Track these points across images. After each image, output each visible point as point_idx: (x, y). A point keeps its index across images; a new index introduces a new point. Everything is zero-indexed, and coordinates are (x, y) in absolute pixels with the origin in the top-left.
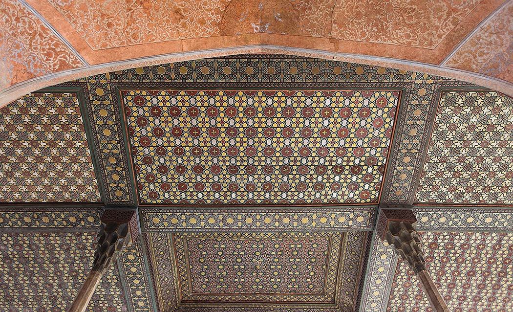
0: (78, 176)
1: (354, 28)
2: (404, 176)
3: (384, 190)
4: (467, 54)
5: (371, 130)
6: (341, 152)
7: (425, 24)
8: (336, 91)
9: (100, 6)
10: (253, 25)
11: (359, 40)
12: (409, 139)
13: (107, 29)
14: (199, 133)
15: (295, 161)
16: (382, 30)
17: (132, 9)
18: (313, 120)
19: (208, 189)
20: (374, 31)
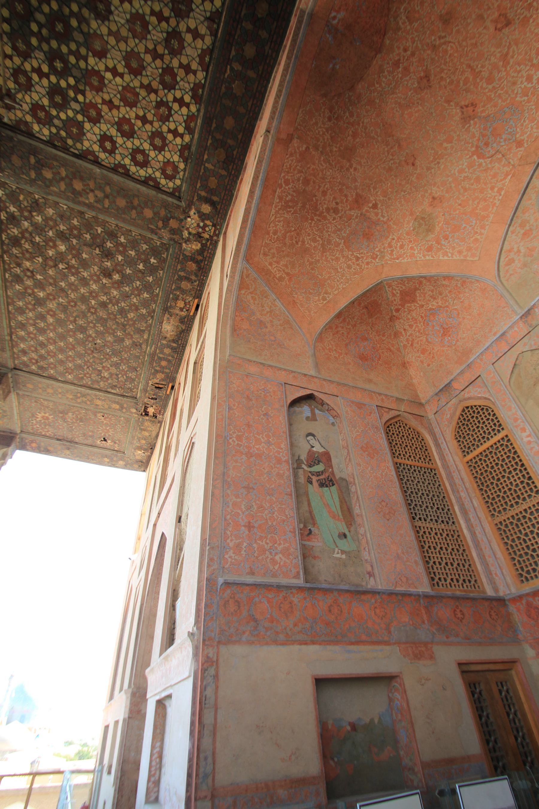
1: (296, 172)
4: (254, 286)
7: (283, 251)
11: (283, 175)
16: (286, 207)
20: (287, 196)
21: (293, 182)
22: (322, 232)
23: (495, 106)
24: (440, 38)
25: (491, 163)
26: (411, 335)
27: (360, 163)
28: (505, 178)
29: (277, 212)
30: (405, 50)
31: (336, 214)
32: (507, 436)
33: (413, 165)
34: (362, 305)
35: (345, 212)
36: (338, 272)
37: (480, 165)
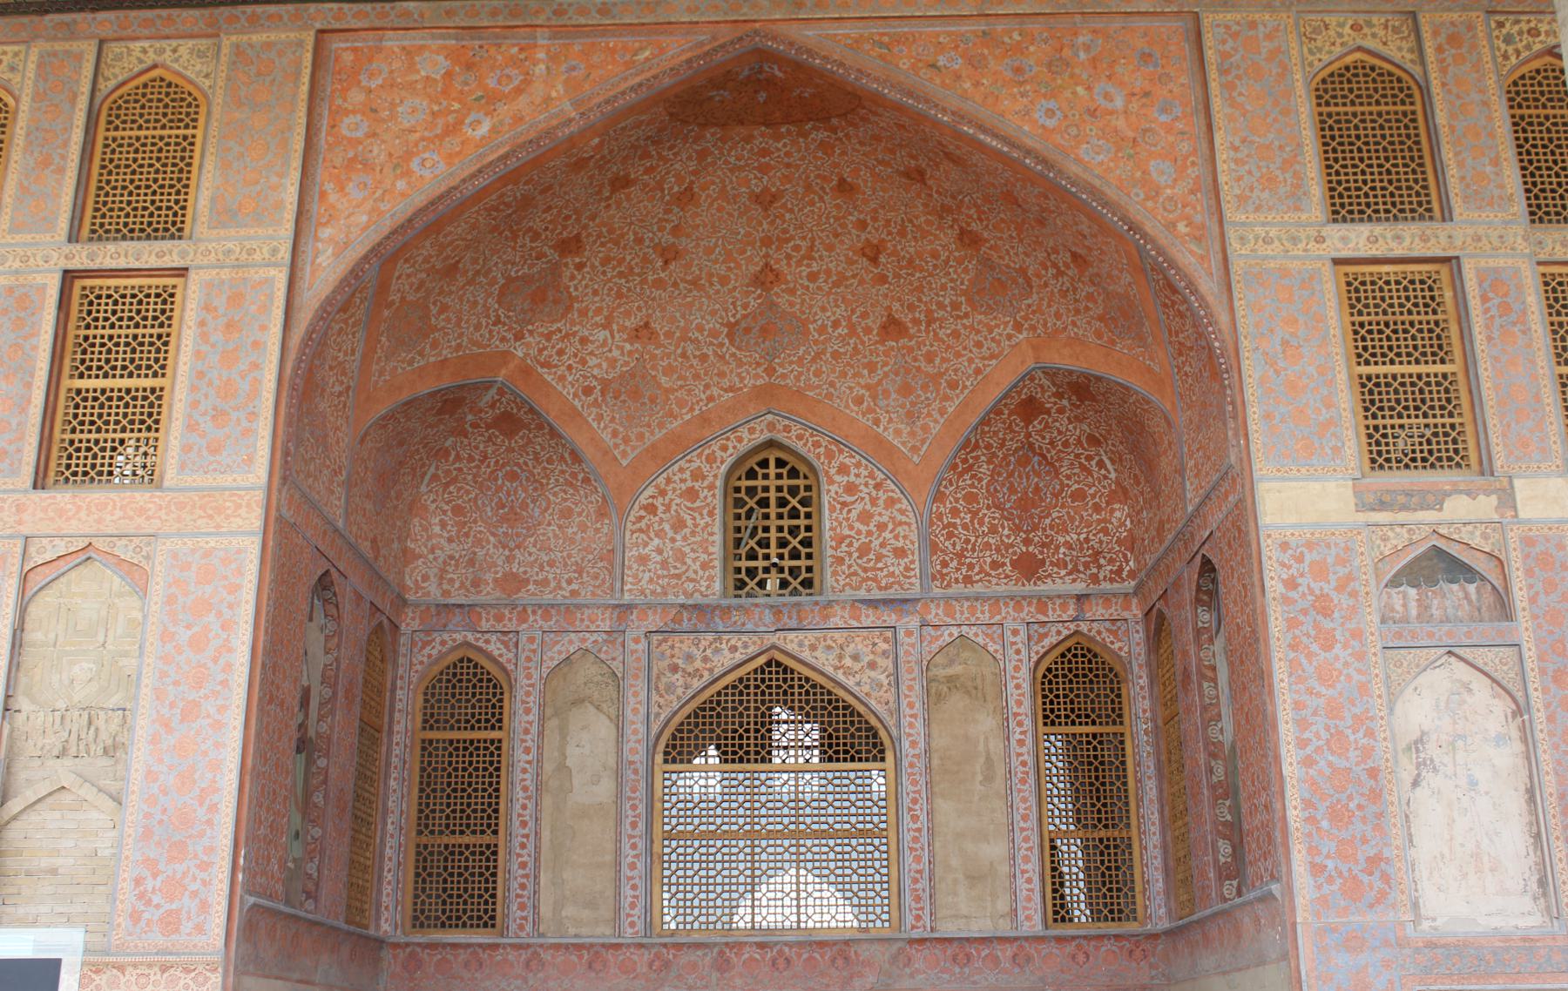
23: (791, 304)
24: (823, 188)
26: (460, 470)
27: (619, 205)
28: (726, 391)
30: (788, 154)
32: (500, 741)
33: (666, 262)
37: (722, 345)
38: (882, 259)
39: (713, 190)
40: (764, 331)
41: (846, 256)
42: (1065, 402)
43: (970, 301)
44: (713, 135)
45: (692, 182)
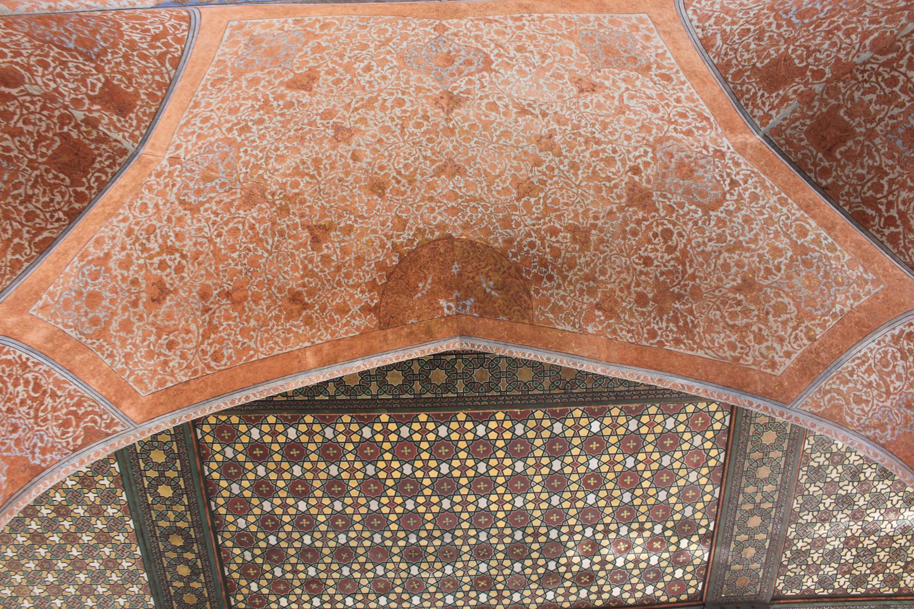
0: (110, 568)
2: (750, 552)
3: (713, 578)
5: (683, 473)
6: (625, 514)
7: (760, 330)
8: (611, 406)
9: (155, 316)
10: (443, 302)
11: (644, 343)
12: (755, 485)
13: (167, 352)
14: (343, 490)
15: (536, 535)
16: (688, 330)
17: (210, 309)
18: (569, 460)
19: (365, 590)
20: (671, 331)
21: (649, 323)
22: (710, 253)
23: (420, 80)
24: (398, 182)
25: (488, 46)
29: (702, 348)
31: (672, 233)
33: (550, 137)
34: (827, 164)
35: (664, 218)
36: (771, 217)
37: (499, 55)
38: (331, 132)
39: (499, 185)
40: (449, 60)
41: (366, 124)
42: (79, 115)
43: (231, 142)
44: (496, 240)
45: (518, 199)
